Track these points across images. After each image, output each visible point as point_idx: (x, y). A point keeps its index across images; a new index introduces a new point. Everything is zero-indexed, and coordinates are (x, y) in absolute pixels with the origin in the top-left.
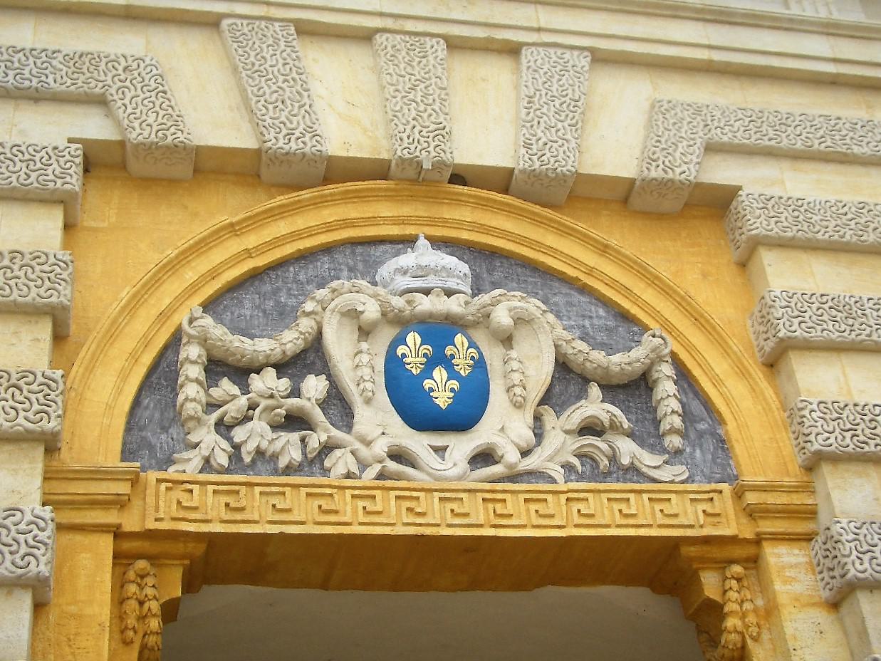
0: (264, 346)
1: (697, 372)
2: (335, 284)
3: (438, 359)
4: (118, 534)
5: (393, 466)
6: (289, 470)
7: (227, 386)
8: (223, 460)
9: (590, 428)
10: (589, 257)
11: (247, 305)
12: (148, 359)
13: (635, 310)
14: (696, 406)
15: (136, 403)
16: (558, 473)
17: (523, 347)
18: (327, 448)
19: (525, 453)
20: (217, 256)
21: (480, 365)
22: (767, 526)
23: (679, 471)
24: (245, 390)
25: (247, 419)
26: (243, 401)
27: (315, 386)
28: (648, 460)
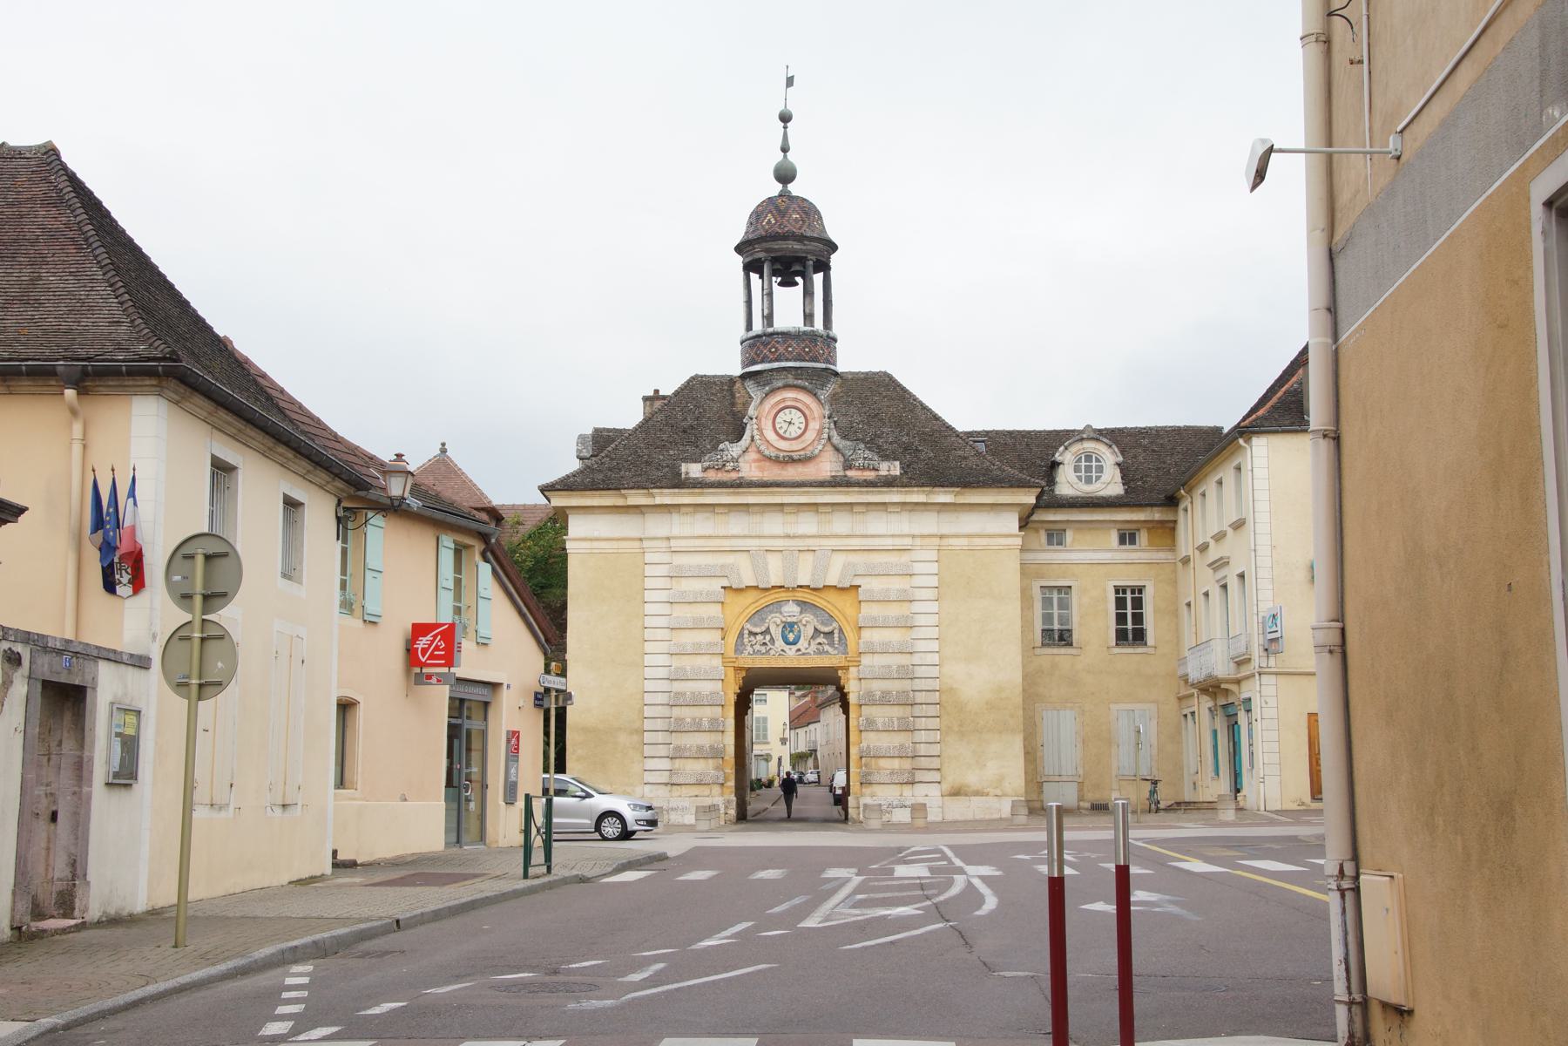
0: (758, 630)
2: (773, 615)
3: (791, 631)
7: (752, 638)
9: (820, 644)
10: (825, 604)
11: (756, 618)
20: (750, 609)
21: (800, 631)
22: (851, 664)
23: (836, 652)
27: (768, 637)
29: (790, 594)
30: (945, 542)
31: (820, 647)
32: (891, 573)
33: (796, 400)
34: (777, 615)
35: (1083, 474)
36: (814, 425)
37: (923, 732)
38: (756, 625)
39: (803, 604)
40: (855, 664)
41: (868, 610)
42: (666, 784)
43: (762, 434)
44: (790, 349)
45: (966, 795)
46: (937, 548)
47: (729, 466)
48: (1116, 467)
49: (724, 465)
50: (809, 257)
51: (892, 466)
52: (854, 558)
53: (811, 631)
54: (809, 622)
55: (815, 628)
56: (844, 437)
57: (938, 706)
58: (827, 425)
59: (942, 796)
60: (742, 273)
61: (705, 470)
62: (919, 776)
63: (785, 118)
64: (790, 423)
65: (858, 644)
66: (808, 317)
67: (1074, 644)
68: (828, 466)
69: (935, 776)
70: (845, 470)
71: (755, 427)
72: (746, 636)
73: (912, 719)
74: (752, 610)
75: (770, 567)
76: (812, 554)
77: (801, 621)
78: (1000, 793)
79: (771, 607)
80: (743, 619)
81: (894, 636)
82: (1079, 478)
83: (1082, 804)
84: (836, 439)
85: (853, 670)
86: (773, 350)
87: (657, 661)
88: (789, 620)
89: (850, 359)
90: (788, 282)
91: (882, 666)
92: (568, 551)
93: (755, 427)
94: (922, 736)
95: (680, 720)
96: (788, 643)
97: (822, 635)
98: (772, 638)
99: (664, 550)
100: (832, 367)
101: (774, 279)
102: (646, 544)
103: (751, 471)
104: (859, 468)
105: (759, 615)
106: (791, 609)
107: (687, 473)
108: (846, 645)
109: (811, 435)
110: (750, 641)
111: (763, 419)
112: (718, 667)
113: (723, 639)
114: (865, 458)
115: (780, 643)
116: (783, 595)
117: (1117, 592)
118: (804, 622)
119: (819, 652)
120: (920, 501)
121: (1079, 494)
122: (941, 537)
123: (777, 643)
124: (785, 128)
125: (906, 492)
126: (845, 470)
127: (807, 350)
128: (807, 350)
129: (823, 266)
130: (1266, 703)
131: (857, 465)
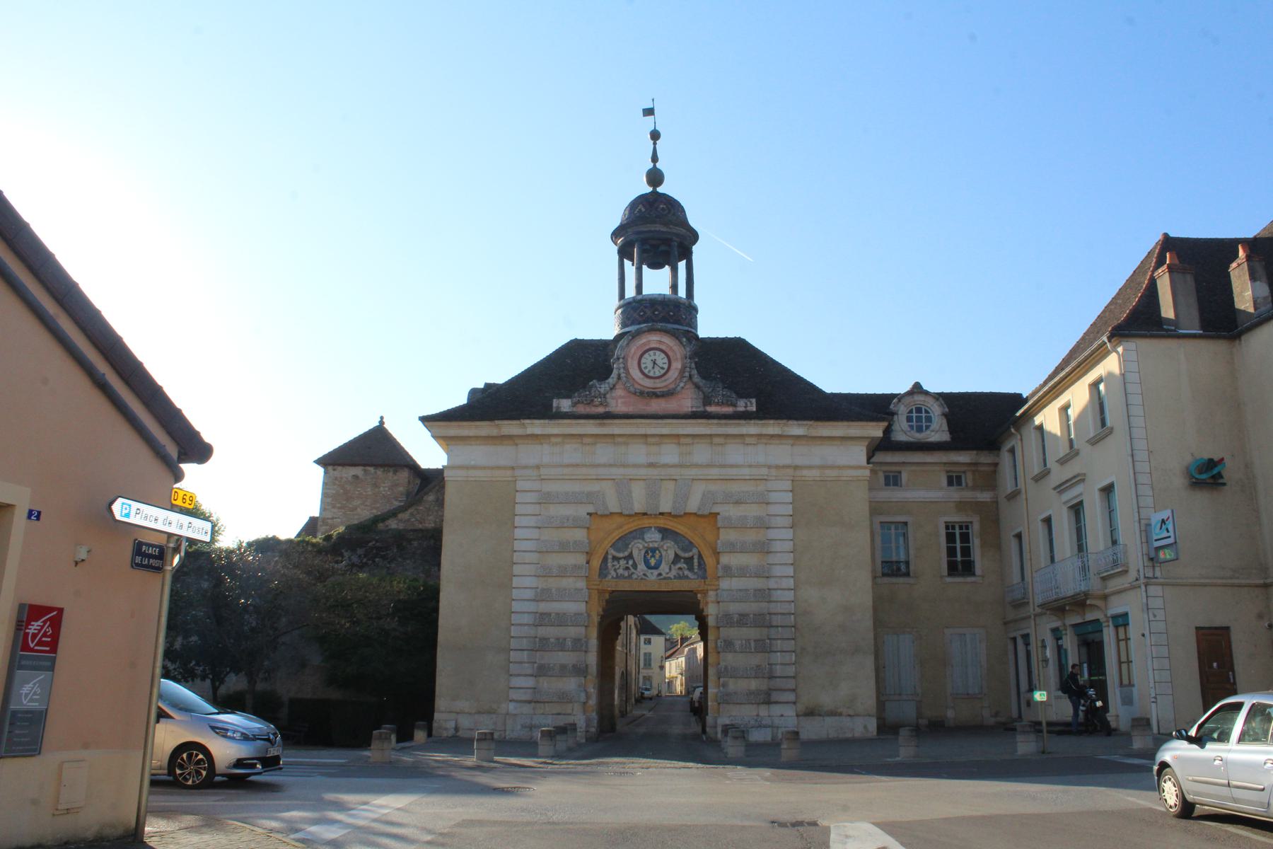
0: (621, 555)
1: (703, 556)
2: (636, 541)
3: (653, 556)
4: (598, 590)
5: (644, 577)
6: (626, 578)
7: (616, 563)
8: (615, 576)
9: (680, 569)
12: (602, 557)
13: (693, 541)
14: (702, 562)
15: (601, 565)
16: (673, 577)
17: (669, 552)
18: (633, 573)
19: (668, 573)
20: (614, 534)
21: (661, 556)
22: (709, 588)
23: (696, 577)
24: (619, 563)
25: (619, 568)
26: (618, 566)
27: (631, 562)
28: (690, 575)
29: (652, 521)
30: (798, 473)
31: (681, 573)
32: (748, 501)
33: (660, 342)
34: (640, 541)
35: (914, 423)
36: (677, 365)
37: (779, 654)
38: (619, 550)
39: (666, 533)
40: (713, 587)
41: (727, 536)
42: (530, 702)
43: (627, 372)
44: (656, 313)
45: (820, 715)
46: (792, 478)
47: (597, 401)
48: (943, 417)
49: (592, 401)
50: (674, 238)
51: (749, 404)
52: (713, 487)
53: (672, 556)
54: (669, 550)
55: (675, 553)
56: (703, 377)
57: (793, 629)
58: (688, 365)
59: (797, 716)
60: (616, 257)
61: (574, 405)
62: (775, 696)
63: (655, 136)
64: (655, 363)
65: (717, 568)
66: (674, 287)
67: (911, 574)
68: (688, 401)
69: (791, 697)
70: (705, 405)
71: (622, 365)
72: (610, 560)
73: (768, 641)
74: (616, 535)
75: (634, 495)
76: (672, 483)
77: (662, 546)
78: (851, 713)
79: (635, 533)
80: (607, 544)
81: (750, 560)
82: (911, 427)
83: (920, 721)
84: (697, 379)
85: (711, 593)
86: (642, 314)
87: (525, 582)
88: (651, 545)
89: (708, 327)
90: (656, 265)
91: (740, 590)
92: (446, 479)
93: (622, 365)
94: (778, 658)
95: (544, 640)
96: (649, 567)
97: (682, 560)
98: (634, 563)
99: (534, 478)
100: (693, 331)
101: (640, 206)
102: (518, 473)
103: (617, 406)
104: (718, 404)
105: (623, 542)
106: (653, 537)
107: (558, 407)
108: (705, 570)
109: (673, 374)
110: (613, 566)
111: (630, 360)
112: (582, 589)
113: (588, 563)
114: (723, 395)
115: (642, 567)
116: (646, 522)
117: (947, 528)
118: (665, 548)
119: (679, 577)
120: (776, 433)
121: (911, 440)
122: (796, 468)
123: (639, 567)
124: (655, 144)
125: (763, 425)
126: (705, 405)
127: (671, 314)
128: (671, 314)
129: (686, 254)
130: (1155, 616)
131: (716, 400)
